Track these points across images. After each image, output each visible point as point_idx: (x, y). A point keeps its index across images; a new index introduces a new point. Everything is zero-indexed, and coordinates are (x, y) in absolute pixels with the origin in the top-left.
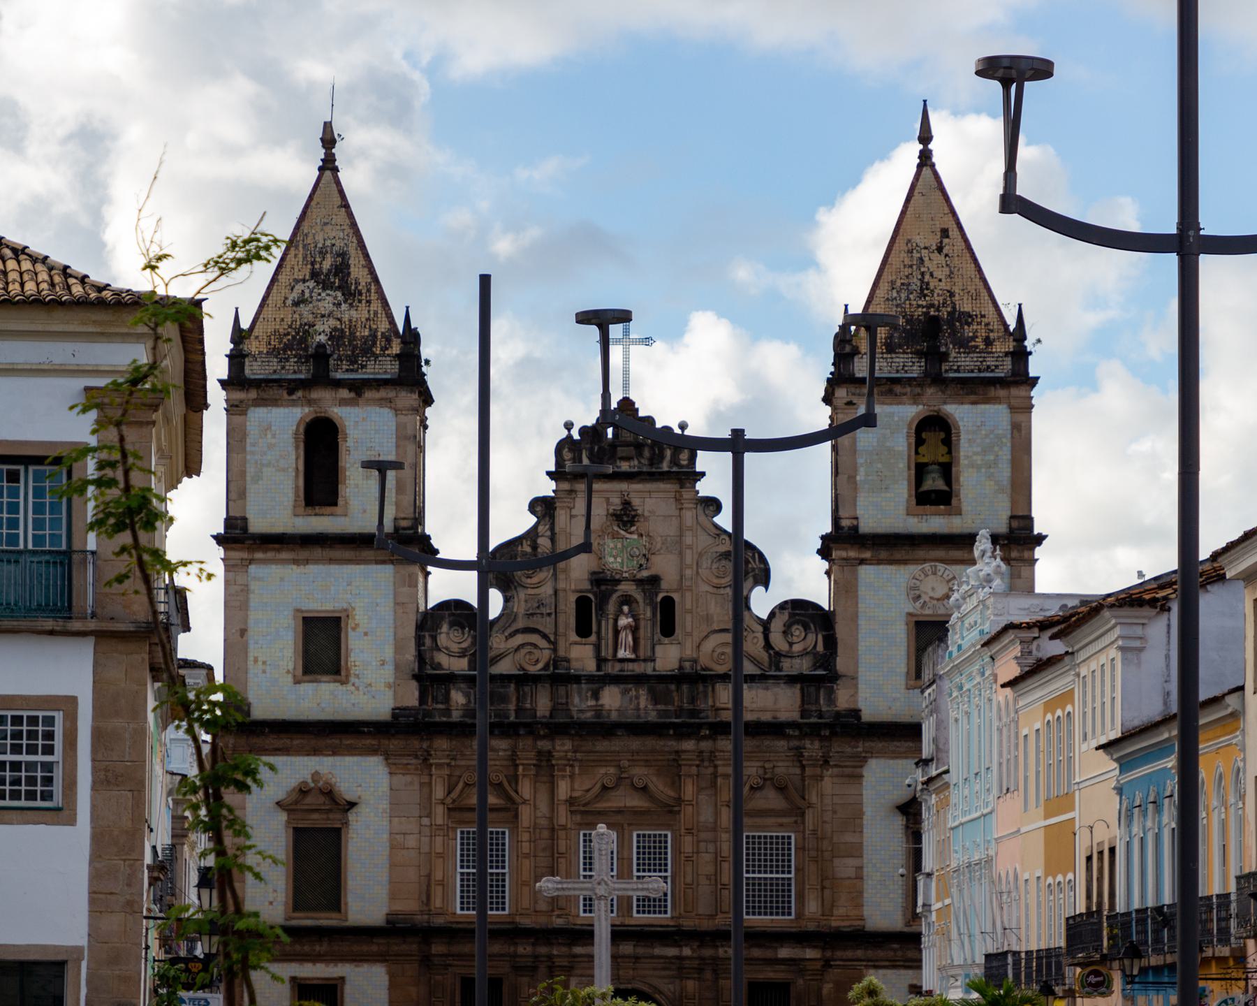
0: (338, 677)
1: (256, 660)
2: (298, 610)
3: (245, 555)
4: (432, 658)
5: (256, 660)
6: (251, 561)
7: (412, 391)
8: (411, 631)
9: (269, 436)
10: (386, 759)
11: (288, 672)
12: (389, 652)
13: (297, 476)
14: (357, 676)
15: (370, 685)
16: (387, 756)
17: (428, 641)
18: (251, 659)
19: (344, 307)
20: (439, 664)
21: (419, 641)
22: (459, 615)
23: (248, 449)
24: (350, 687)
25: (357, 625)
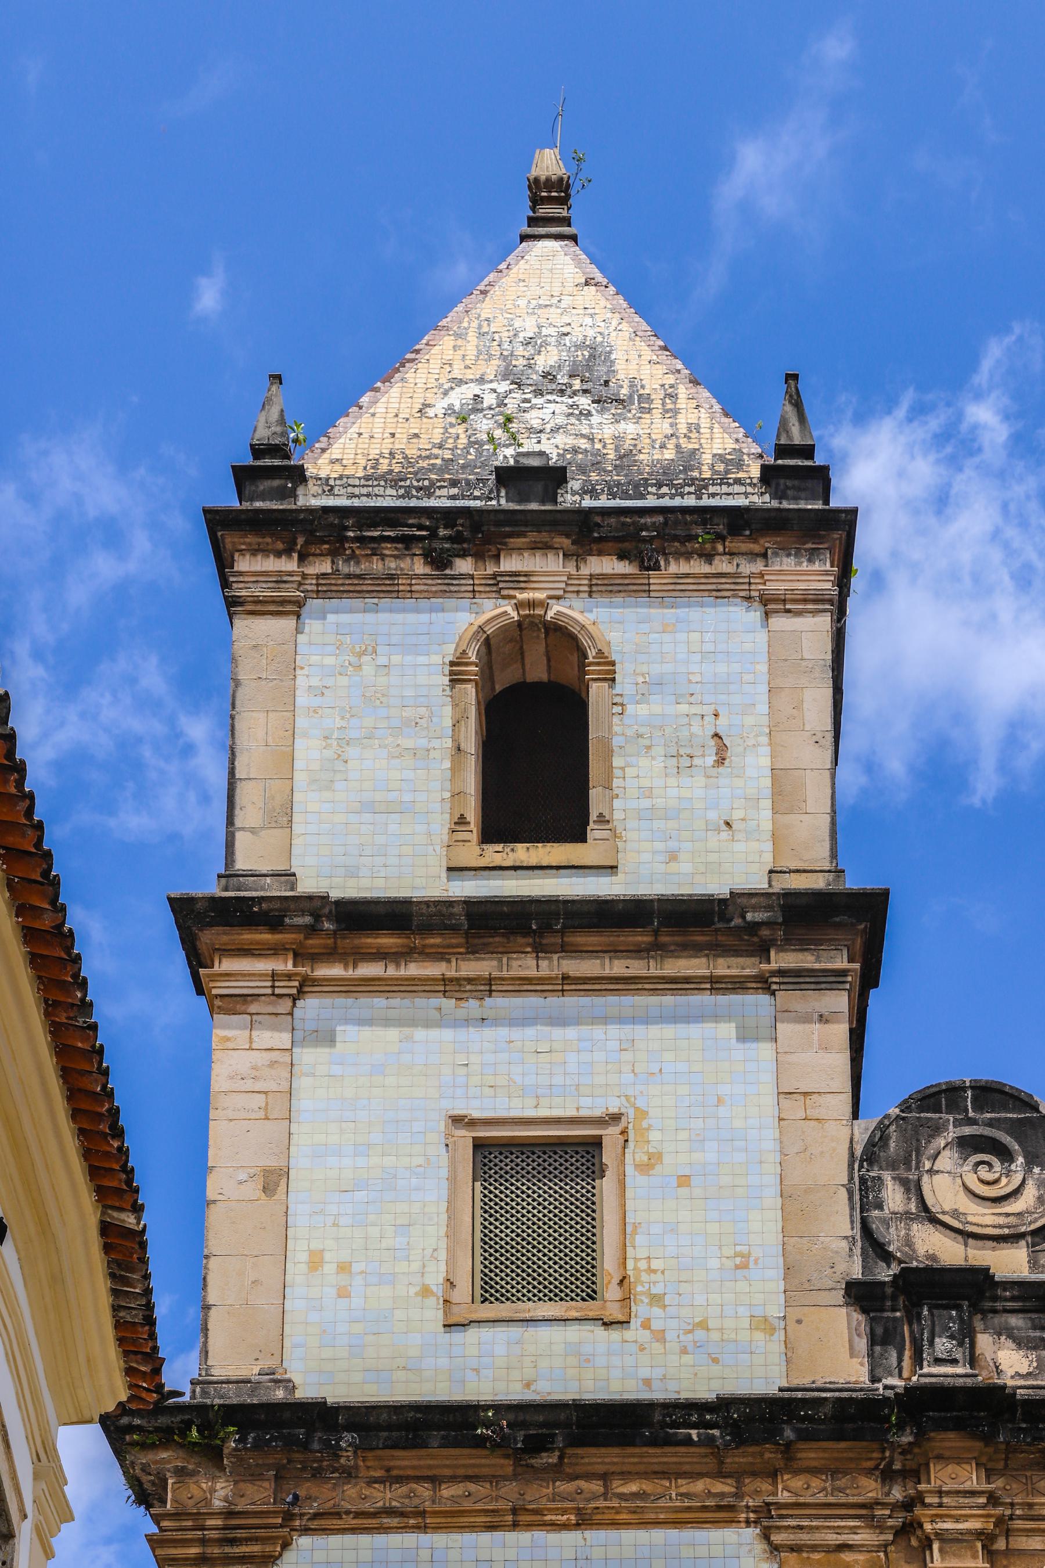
0: (592, 1308)
1: (316, 1261)
2: (457, 1120)
3: (285, 965)
4: (909, 1242)
5: (316, 1261)
6: (305, 986)
7: (812, 555)
8: (835, 1170)
9: (368, 670)
10: (766, 1536)
11: (426, 1291)
12: (763, 1229)
13: (456, 769)
14: (657, 1300)
15: (703, 1325)
16: (765, 1519)
17: (893, 1197)
18: (299, 1255)
19: (596, 419)
20: (933, 1257)
21: (865, 1195)
22: (990, 1123)
23: (302, 699)
24: (634, 1333)
25: (654, 1160)
